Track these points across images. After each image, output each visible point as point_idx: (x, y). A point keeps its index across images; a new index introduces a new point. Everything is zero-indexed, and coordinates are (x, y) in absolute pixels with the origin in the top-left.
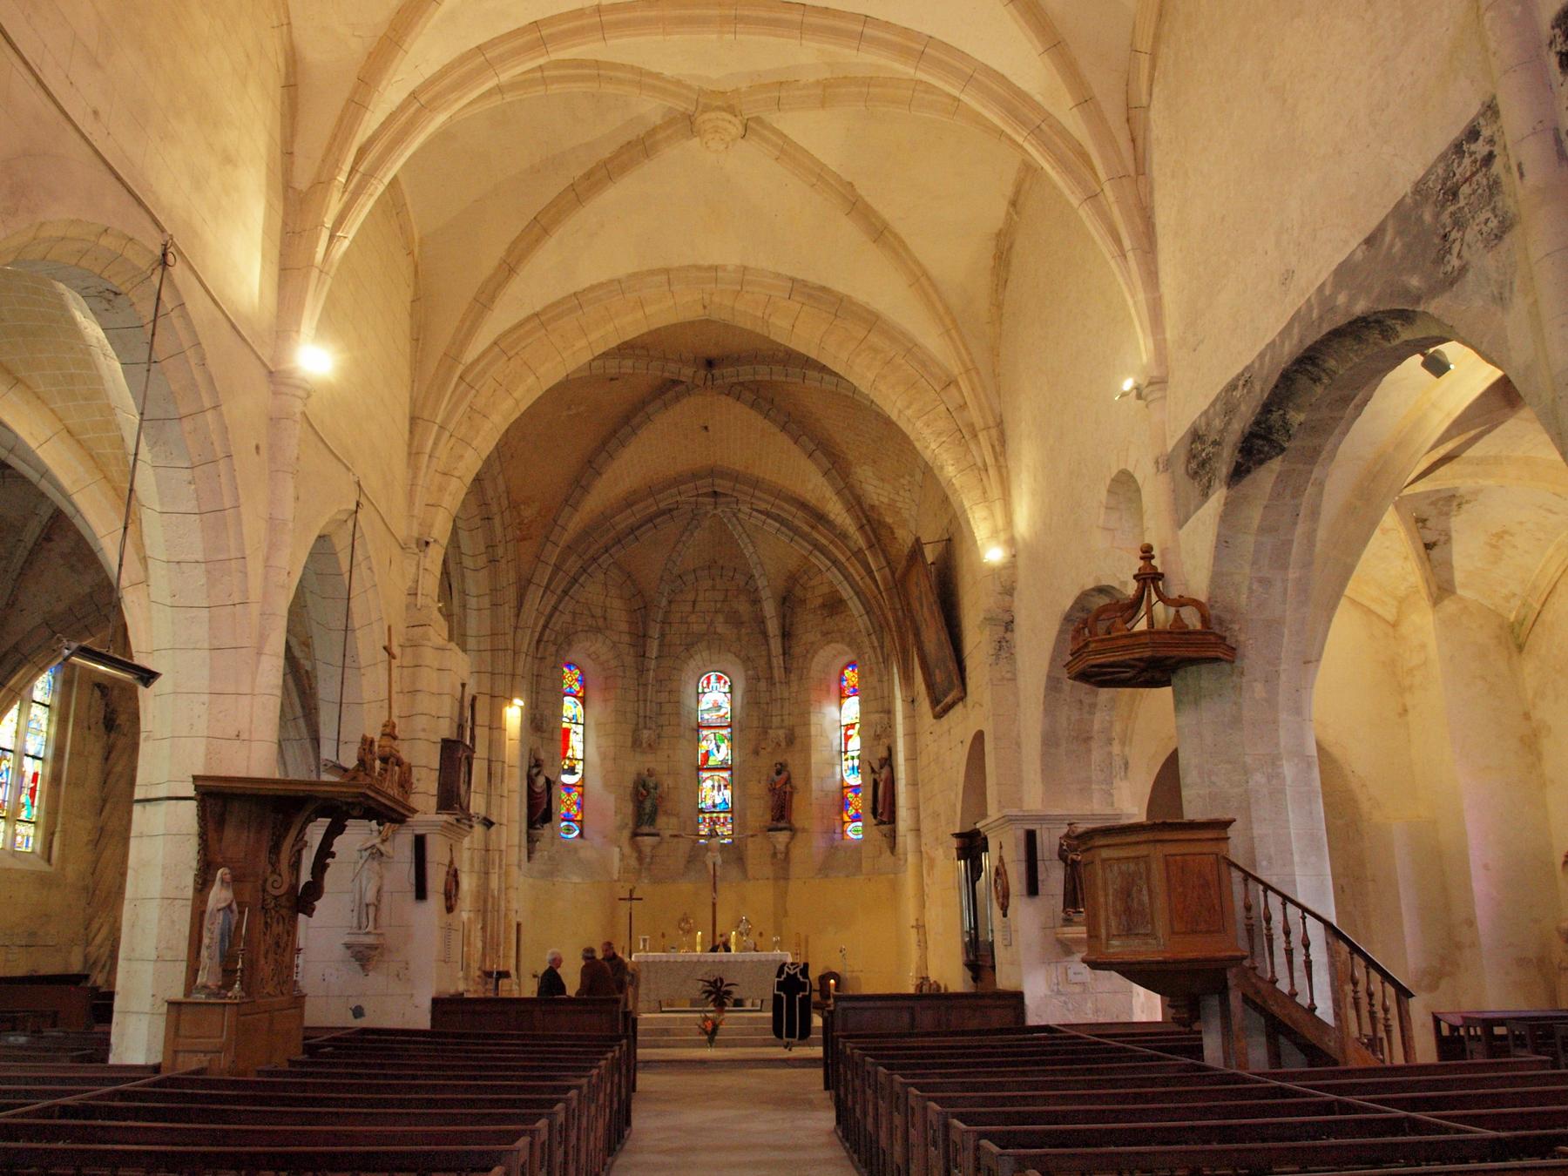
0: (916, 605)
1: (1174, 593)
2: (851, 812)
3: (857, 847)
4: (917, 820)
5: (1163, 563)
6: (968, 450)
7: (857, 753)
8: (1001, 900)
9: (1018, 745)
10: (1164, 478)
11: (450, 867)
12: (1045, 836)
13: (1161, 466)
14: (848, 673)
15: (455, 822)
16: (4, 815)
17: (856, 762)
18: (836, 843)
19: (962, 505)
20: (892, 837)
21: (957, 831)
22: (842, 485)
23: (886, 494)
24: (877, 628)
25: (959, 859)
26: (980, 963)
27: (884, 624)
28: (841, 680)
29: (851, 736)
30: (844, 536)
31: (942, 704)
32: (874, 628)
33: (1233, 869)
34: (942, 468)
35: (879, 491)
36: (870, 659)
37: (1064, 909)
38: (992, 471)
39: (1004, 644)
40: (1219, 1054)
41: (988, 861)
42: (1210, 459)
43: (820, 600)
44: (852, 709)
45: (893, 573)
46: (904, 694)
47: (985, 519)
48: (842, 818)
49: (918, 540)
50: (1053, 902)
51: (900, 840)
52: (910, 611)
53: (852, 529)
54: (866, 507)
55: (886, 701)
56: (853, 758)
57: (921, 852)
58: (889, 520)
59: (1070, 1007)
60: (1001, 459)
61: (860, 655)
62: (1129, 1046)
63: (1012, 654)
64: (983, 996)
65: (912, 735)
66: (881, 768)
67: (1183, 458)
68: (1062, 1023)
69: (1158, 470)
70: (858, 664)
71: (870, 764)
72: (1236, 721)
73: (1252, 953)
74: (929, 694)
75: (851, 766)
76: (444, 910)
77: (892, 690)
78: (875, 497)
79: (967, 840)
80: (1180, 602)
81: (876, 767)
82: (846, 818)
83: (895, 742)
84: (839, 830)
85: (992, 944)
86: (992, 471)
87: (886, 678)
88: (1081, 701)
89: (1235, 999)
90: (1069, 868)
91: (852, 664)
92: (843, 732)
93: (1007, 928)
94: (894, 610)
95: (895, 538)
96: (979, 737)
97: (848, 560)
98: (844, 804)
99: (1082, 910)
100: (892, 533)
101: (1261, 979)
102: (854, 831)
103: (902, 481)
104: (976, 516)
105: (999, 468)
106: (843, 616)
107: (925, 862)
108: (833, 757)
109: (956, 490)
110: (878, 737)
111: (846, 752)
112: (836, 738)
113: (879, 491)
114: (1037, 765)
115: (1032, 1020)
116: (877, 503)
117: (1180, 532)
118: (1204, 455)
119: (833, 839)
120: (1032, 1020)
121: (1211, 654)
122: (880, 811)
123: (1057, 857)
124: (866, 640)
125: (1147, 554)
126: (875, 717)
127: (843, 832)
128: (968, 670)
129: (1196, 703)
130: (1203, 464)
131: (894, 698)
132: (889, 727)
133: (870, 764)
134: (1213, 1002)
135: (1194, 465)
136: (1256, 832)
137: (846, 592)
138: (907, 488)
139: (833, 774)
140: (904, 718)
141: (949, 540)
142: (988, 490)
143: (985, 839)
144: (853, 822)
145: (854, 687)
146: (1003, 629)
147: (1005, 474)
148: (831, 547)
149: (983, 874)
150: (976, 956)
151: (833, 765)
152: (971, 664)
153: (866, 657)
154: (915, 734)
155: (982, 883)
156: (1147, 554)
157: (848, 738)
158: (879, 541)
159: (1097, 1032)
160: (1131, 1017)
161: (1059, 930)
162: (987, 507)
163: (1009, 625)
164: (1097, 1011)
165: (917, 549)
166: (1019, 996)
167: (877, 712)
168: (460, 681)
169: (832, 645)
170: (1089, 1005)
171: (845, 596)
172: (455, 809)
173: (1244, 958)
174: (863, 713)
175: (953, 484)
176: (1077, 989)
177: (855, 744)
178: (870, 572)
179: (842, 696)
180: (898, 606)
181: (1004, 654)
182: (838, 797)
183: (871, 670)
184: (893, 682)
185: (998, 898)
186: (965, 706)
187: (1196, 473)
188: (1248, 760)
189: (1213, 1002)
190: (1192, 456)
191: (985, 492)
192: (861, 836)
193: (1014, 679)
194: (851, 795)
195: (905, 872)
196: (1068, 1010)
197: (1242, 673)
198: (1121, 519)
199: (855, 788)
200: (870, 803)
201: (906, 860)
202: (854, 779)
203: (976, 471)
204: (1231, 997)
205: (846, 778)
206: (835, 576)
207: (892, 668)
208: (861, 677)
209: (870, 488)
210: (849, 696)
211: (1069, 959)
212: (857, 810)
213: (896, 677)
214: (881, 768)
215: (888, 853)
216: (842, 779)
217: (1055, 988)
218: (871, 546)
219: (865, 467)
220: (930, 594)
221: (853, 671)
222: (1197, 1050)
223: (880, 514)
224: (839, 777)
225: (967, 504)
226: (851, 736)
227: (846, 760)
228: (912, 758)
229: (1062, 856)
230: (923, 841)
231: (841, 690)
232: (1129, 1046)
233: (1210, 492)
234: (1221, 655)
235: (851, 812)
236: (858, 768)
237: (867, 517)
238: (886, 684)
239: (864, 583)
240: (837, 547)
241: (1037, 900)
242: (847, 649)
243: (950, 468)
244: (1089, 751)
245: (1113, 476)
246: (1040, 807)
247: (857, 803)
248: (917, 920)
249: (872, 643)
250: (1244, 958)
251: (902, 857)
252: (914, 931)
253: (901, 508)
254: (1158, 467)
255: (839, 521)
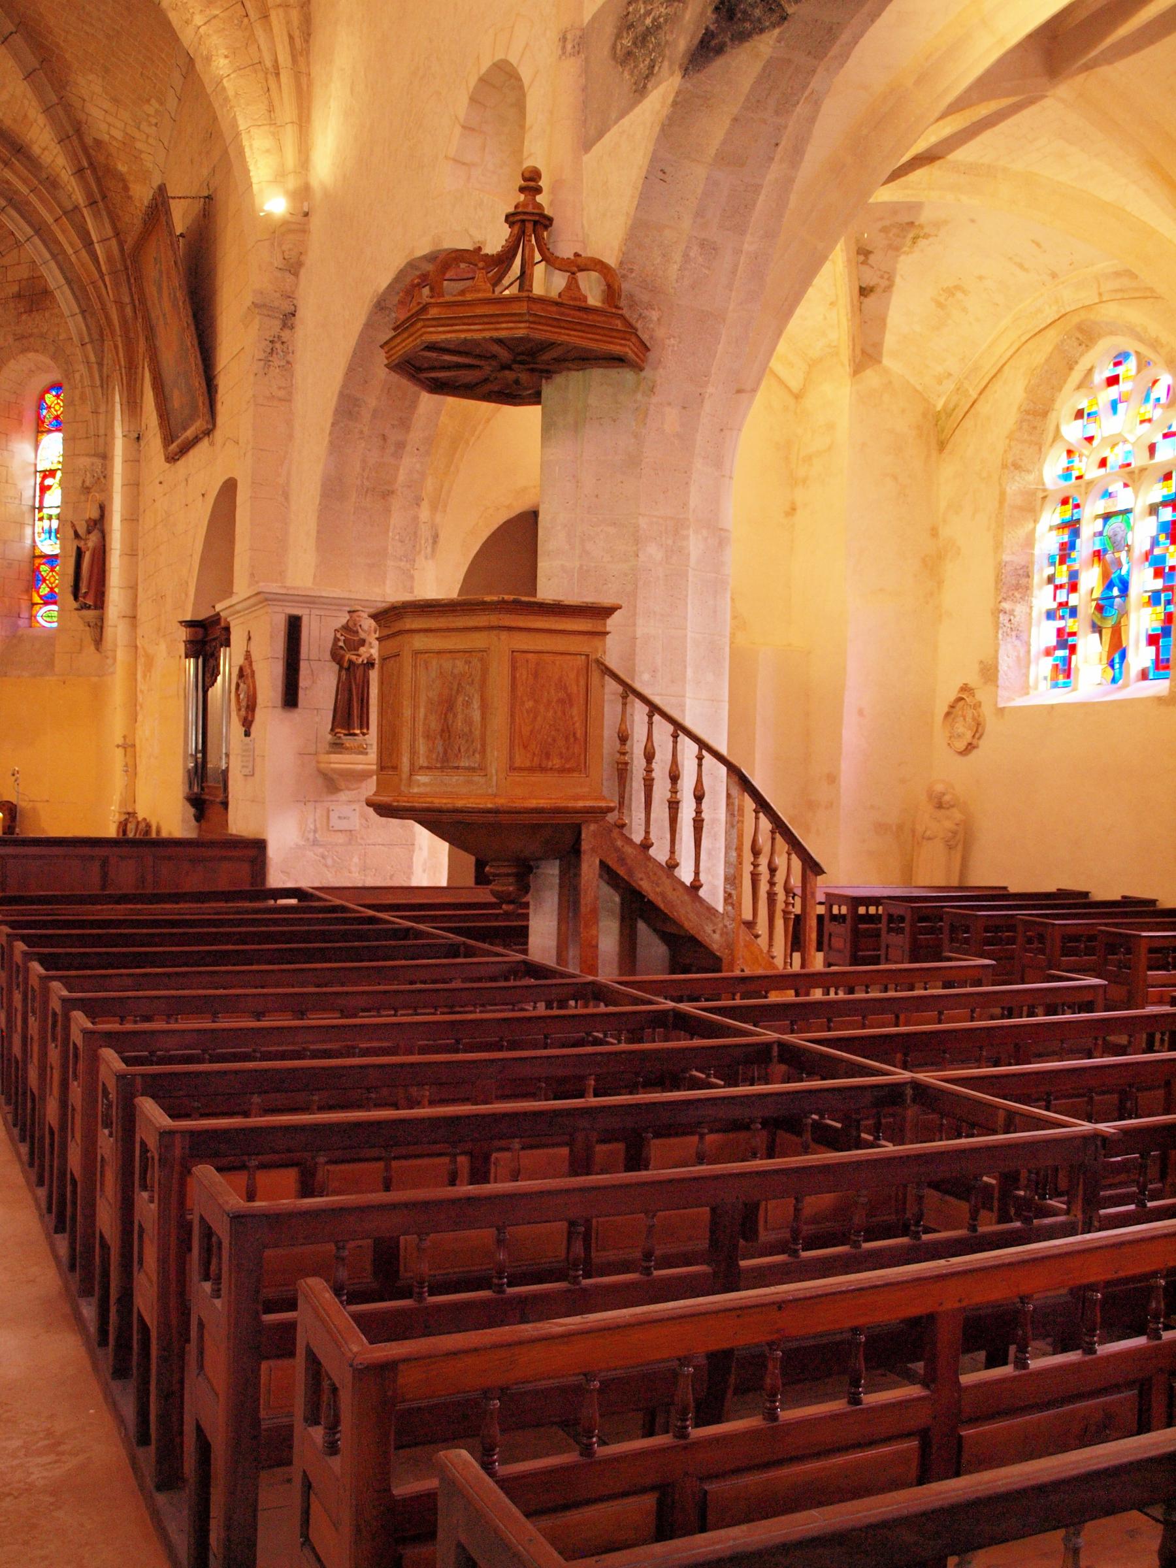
0: (151, 290)
1: (565, 250)
2: (44, 590)
3: (50, 638)
4: (134, 605)
5: (552, 203)
6: (252, 38)
7: (58, 511)
8: (243, 712)
9: (286, 495)
10: (571, 66)
12: (315, 625)
13: (569, 46)
14: (50, 398)
17: (55, 524)
18: (20, 633)
19: (234, 124)
20: (99, 627)
21: (188, 618)
22: (54, 98)
23: (120, 125)
24: (96, 336)
25: (186, 657)
26: (207, 797)
27: (103, 321)
28: (40, 408)
29: (49, 487)
30: (53, 184)
31: (179, 441)
32: (90, 334)
33: (608, 679)
34: (208, 59)
35: (110, 119)
36: (81, 381)
37: (332, 730)
38: (285, 77)
39: (278, 345)
40: (552, 943)
41: (228, 662)
42: (659, 27)
43: (15, 289)
44: (52, 449)
45: (121, 244)
46: (126, 429)
47: (268, 151)
48: (31, 599)
49: (162, 189)
50: (317, 719)
51: (109, 632)
52: (143, 301)
53: (66, 176)
54: (89, 141)
55: (101, 440)
56: (50, 518)
57: (136, 647)
58: (122, 168)
59: (329, 862)
60: (301, 60)
61: (68, 374)
62: (421, 927)
63: (288, 362)
64: (211, 844)
65: (134, 486)
66: (89, 532)
67: (609, 29)
68: (317, 885)
69: (564, 53)
70: (66, 387)
71: (73, 526)
72: (633, 462)
73: (621, 804)
74: (161, 425)
75: (46, 527)
77: (110, 426)
78: (104, 127)
79: (200, 631)
80: (576, 266)
81: (82, 531)
82: (37, 599)
83: (110, 498)
84: (25, 614)
85: (225, 773)
86: (285, 77)
87: (102, 409)
88: (384, 438)
89: (589, 868)
90: (344, 672)
91: (57, 386)
92: (39, 480)
93: (249, 754)
94: (119, 304)
95: (130, 198)
96: (230, 487)
97: (56, 220)
98: (35, 578)
99: (358, 732)
100: (126, 188)
101: (629, 841)
102: (47, 617)
103: (146, 107)
104: (257, 144)
105: (297, 75)
106: (47, 314)
107: (141, 661)
108: (23, 514)
109: (226, 100)
110: (86, 490)
111: (41, 509)
112: (28, 488)
113: (110, 119)
114: (312, 525)
115: (276, 880)
116: (106, 138)
117: (586, 158)
118: (648, 21)
119: (16, 627)
120: (276, 880)
121: (616, 349)
122: (83, 590)
123: (328, 656)
124: (78, 351)
125: (531, 183)
126: (84, 462)
127: (32, 617)
128: (221, 390)
129: (576, 427)
130: (642, 40)
131: (113, 438)
132: (102, 479)
133: (73, 526)
134: (551, 871)
135: (627, 42)
136: (639, 633)
137: (54, 278)
138: (154, 121)
139: (21, 538)
140: (125, 461)
141: (209, 198)
142: (276, 103)
143: (227, 629)
144: (46, 603)
145: (56, 418)
146: (277, 324)
147: (305, 87)
148: (33, 198)
149: (219, 678)
150: (202, 789)
151: (22, 525)
152: (224, 383)
153: (77, 376)
154: (138, 485)
155: (217, 690)
156: (531, 183)
157: (44, 489)
158: (104, 197)
159: (368, 902)
160: (409, 878)
161: (324, 758)
162: (273, 134)
163: (288, 319)
164: (364, 869)
165: (160, 205)
166: (259, 846)
167: (87, 455)
169: (31, 355)
170: (356, 860)
171: (52, 285)
173: (610, 810)
174: (69, 454)
175: (224, 89)
176: (341, 838)
177: (54, 498)
178: (88, 244)
179: (40, 428)
180: (127, 300)
181: (276, 361)
182: (26, 567)
183: (83, 398)
184: (113, 413)
185: (239, 710)
186: (212, 444)
187: (629, 54)
188: (643, 522)
189: (551, 871)
190: (626, 24)
191: (271, 109)
192: (55, 625)
193: (288, 399)
194: (44, 569)
195: (113, 673)
196: (326, 866)
197: (652, 390)
198: (483, 148)
199: (51, 559)
200: (70, 579)
201: (115, 659)
202: (49, 546)
203: (261, 75)
204: (585, 867)
205: (39, 544)
206: (36, 250)
207: (113, 394)
208: (69, 404)
209: (96, 113)
210: (49, 431)
211: (334, 798)
212: (52, 589)
213: (118, 407)
214: (89, 532)
215: (92, 648)
216: (34, 546)
217: (311, 836)
218: (92, 203)
219: (91, 77)
220: (174, 272)
221: (57, 396)
222: (520, 935)
223: (109, 155)
224: (28, 542)
225: (242, 125)
226: (49, 487)
227: (41, 519)
228: (132, 518)
229: (336, 656)
230: (140, 632)
231: (40, 420)
232: (421, 927)
233: (649, 86)
234: (631, 355)
235: (44, 590)
236: (57, 531)
237: (89, 157)
238: (102, 417)
239: (78, 258)
240: (42, 200)
241: (296, 715)
242: (48, 361)
243: (222, 62)
244: (388, 511)
245: (483, 70)
246: (309, 584)
247: (56, 579)
248: (125, 737)
249: (87, 357)
250: (610, 810)
251: (110, 654)
252: (120, 751)
253: (141, 152)
254: (564, 48)
255: (46, 159)
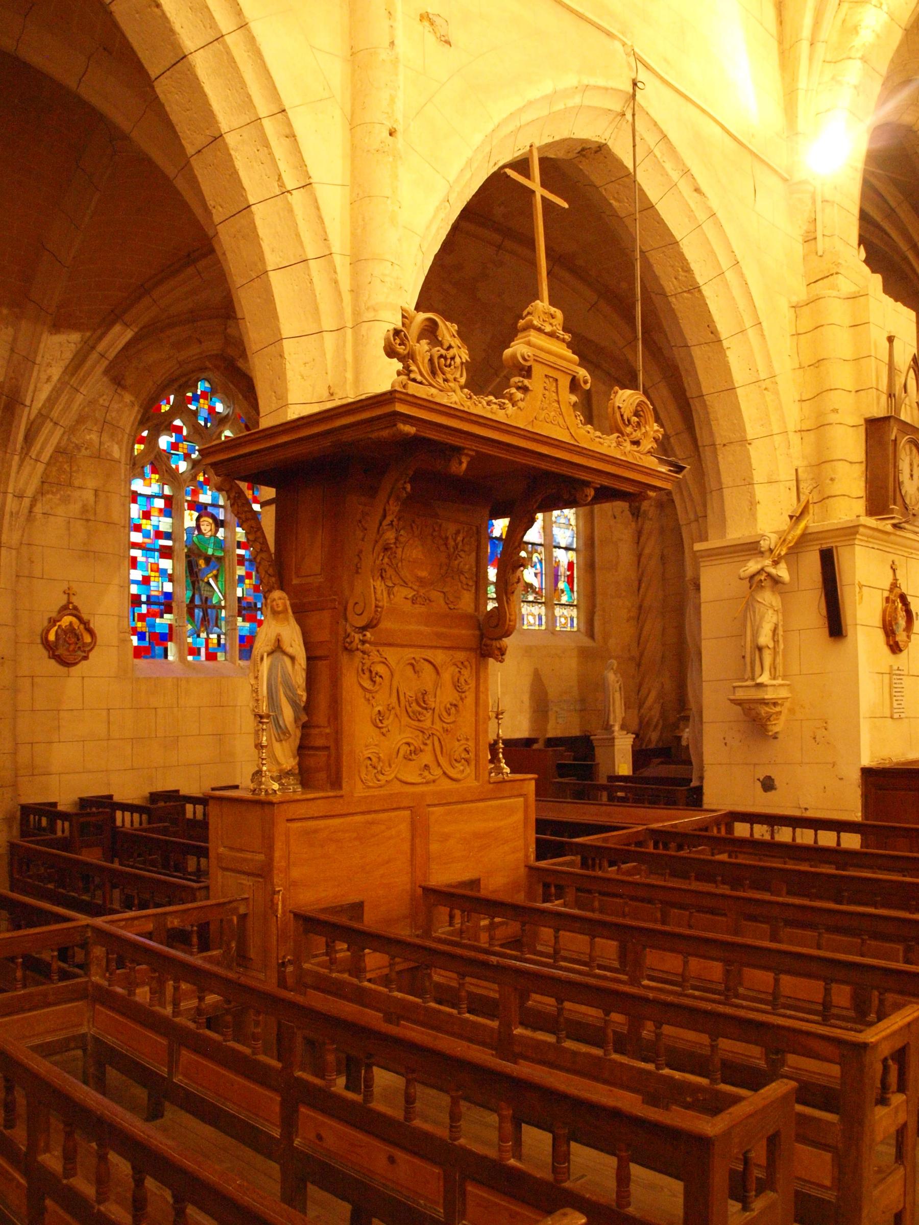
11: (891, 591)
15: (889, 528)
16: (543, 600)
76: (886, 650)
168: (886, 335)
172: (892, 511)
